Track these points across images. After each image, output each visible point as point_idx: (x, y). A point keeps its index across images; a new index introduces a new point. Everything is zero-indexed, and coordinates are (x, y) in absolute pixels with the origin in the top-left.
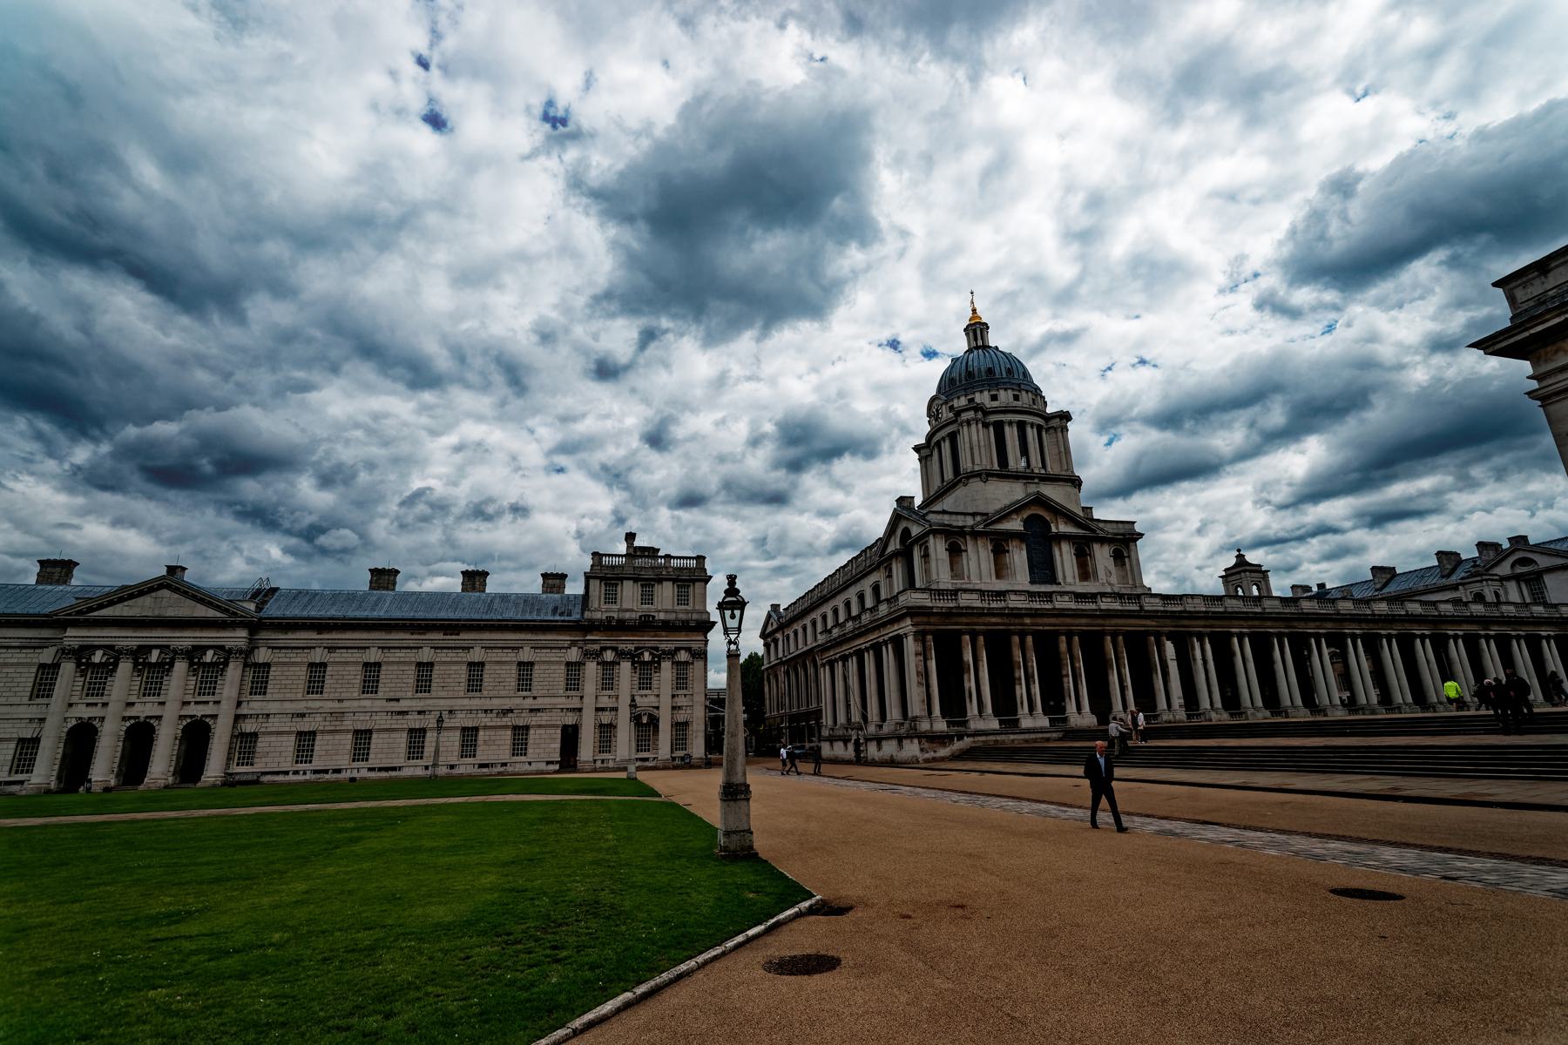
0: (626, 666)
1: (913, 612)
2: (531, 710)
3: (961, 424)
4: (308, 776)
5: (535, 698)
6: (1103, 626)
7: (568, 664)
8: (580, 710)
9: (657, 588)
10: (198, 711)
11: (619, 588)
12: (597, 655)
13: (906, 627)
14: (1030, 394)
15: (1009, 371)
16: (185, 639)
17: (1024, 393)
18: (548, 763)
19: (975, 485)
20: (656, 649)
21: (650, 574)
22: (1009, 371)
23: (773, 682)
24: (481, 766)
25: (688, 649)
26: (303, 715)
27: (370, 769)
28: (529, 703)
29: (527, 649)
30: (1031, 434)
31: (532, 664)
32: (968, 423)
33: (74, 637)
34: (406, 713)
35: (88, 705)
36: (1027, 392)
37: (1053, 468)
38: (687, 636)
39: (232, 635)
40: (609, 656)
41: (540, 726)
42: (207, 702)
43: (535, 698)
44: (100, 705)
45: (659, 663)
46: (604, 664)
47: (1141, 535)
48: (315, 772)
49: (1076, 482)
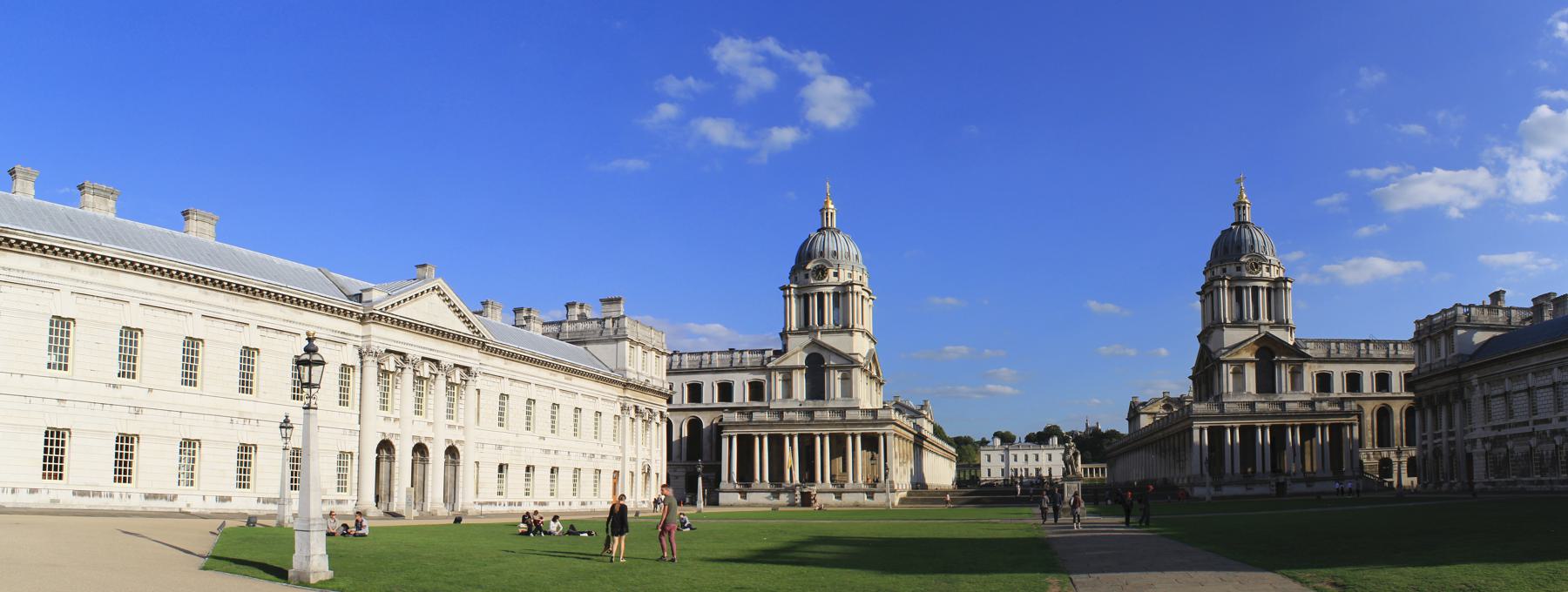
4: (506, 509)
10: (455, 436)
16: (449, 353)
20: (651, 410)
24: (583, 504)
25: (661, 413)
26: (500, 447)
27: (535, 503)
28: (599, 450)
33: (383, 336)
34: (547, 451)
35: (386, 418)
39: (470, 356)
42: (455, 426)
44: (392, 420)
48: (510, 504)
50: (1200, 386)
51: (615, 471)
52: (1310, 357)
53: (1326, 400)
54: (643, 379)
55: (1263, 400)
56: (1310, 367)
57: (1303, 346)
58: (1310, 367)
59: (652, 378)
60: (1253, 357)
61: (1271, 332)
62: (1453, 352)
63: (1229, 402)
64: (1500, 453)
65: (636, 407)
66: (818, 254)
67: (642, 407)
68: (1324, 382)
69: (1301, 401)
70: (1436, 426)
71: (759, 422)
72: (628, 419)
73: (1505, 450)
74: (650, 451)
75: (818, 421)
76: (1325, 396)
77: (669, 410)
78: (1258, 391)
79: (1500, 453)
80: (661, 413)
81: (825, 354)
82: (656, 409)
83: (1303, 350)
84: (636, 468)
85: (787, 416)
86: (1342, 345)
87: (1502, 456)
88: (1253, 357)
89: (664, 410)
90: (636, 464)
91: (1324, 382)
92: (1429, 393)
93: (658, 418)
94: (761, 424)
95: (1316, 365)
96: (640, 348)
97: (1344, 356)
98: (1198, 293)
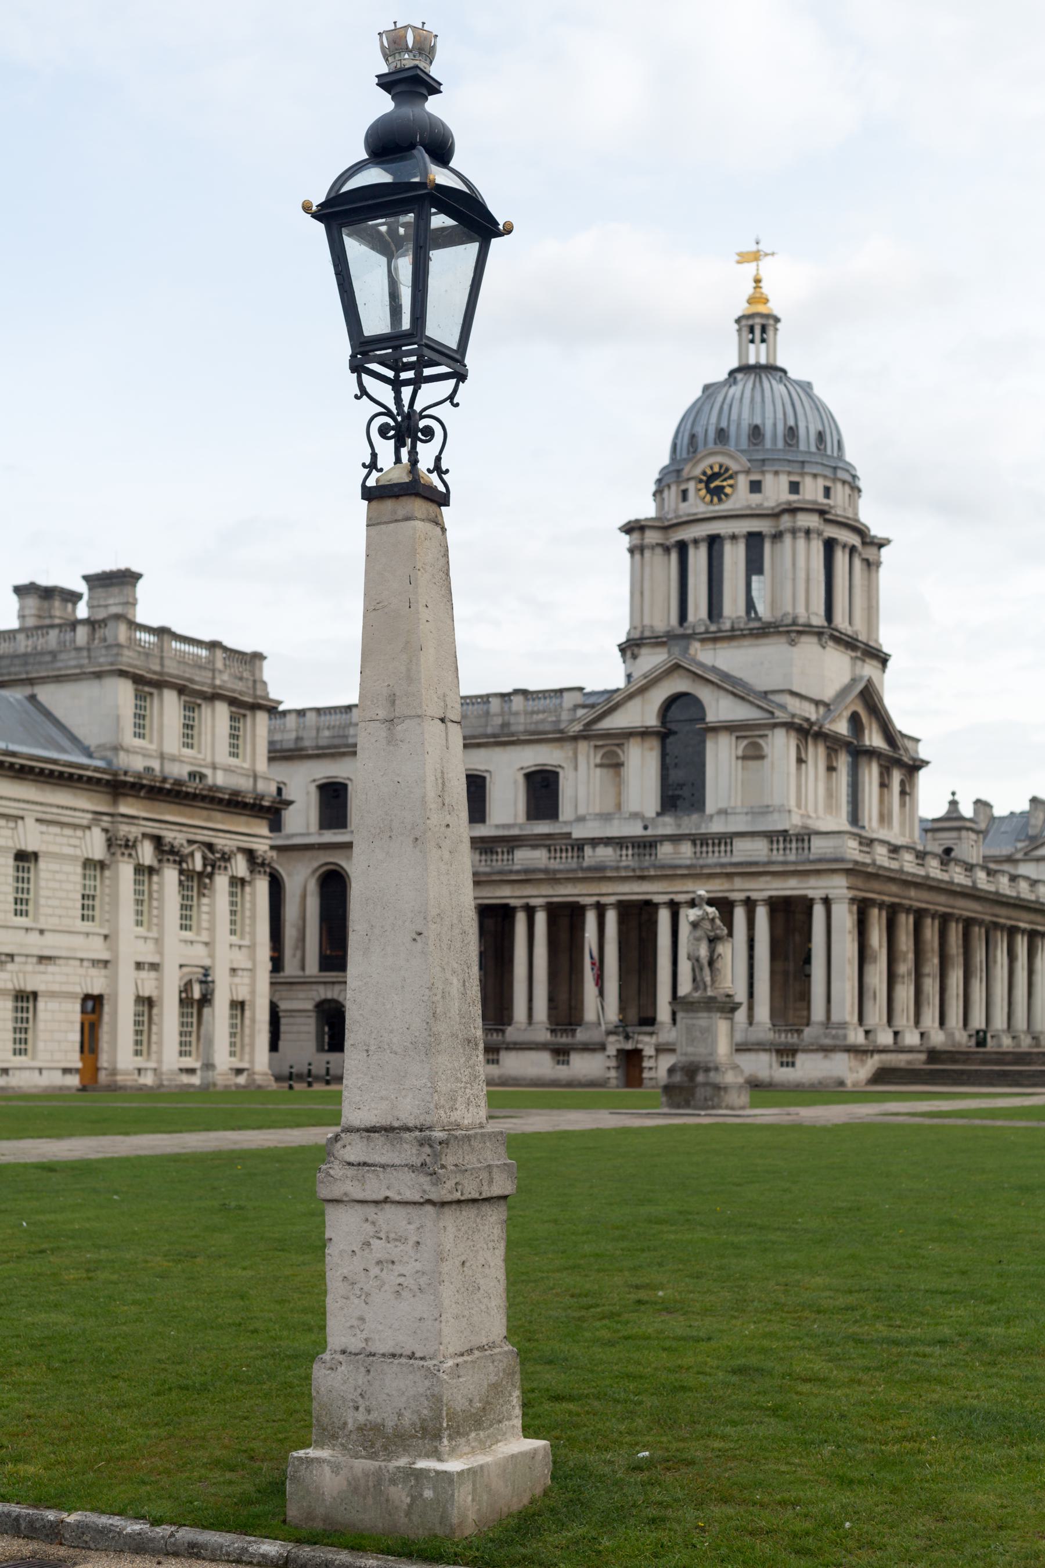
0: (171, 875)
1: (855, 871)
2: (42, 959)
3: (794, 532)
5: (42, 932)
6: (953, 907)
7: (88, 863)
8: (106, 963)
9: (206, 710)
11: (249, 720)
12: (129, 846)
13: (838, 887)
14: (847, 488)
15: (821, 436)
17: (839, 486)
18: (66, 1071)
19: (809, 646)
20: (210, 846)
21: (202, 680)
22: (821, 436)
23: (956, 977)
25: (250, 854)
28: (35, 944)
29: (30, 822)
30: (841, 559)
31: (35, 856)
32: (808, 532)
36: (844, 482)
37: (859, 629)
38: (208, 819)
40: (147, 853)
41: (53, 995)
43: (42, 932)
45: (211, 876)
46: (139, 869)
47: (925, 763)
49: (883, 660)
51: (87, 997)
54: (179, 771)
59: (214, 767)
65: (158, 841)
66: (712, 434)
67: (173, 837)
71: (526, 871)
72: (126, 871)
74: (158, 941)
75: (663, 867)
77: (272, 848)
80: (250, 854)
81: (705, 694)
82: (222, 842)
84: (160, 987)
85: (593, 856)
89: (262, 847)
90: (160, 980)
93: (240, 867)
94: (528, 877)
96: (170, 698)
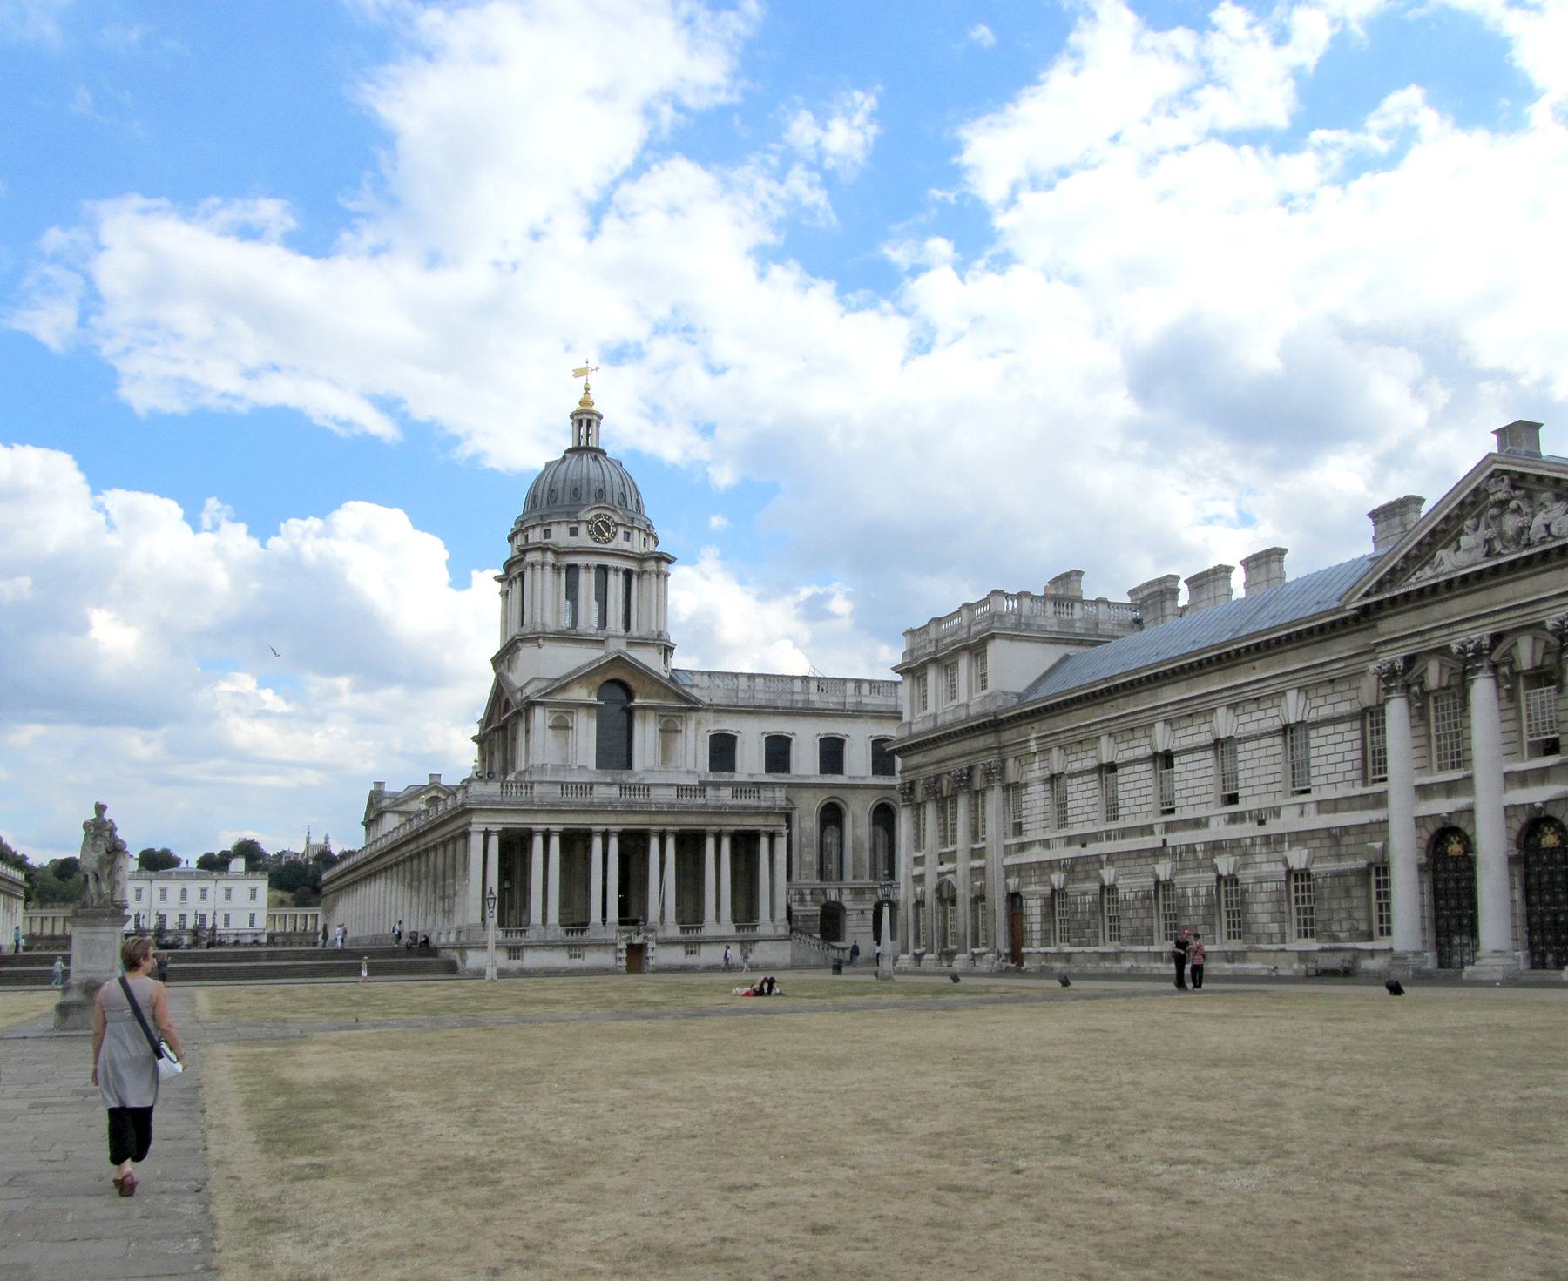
50: (492, 753)
52: (699, 701)
53: (727, 784)
55: (609, 780)
56: (698, 723)
57: (687, 682)
58: (698, 723)
60: (594, 699)
61: (632, 654)
62: (953, 698)
63: (541, 783)
64: (1085, 894)
68: (723, 750)
69: (678, 786)
70: (948, 833)
73: (1096, 886)
76: (725, 776)
78: (598, 766)
79: (1085, 894)
83: (687, 689)
86: (759, 681)
87: (1089, 898)
88: (594, 699)
91: (723, 750)
92: (931, 771)
95: (710, 716)
97: (763, 703)
98: (498, 579)
